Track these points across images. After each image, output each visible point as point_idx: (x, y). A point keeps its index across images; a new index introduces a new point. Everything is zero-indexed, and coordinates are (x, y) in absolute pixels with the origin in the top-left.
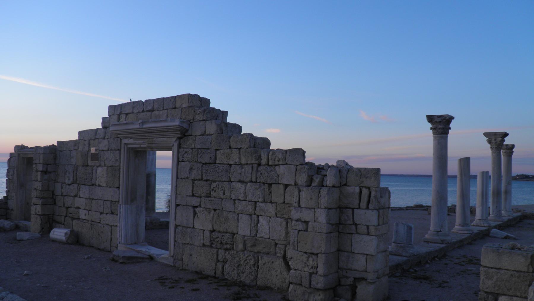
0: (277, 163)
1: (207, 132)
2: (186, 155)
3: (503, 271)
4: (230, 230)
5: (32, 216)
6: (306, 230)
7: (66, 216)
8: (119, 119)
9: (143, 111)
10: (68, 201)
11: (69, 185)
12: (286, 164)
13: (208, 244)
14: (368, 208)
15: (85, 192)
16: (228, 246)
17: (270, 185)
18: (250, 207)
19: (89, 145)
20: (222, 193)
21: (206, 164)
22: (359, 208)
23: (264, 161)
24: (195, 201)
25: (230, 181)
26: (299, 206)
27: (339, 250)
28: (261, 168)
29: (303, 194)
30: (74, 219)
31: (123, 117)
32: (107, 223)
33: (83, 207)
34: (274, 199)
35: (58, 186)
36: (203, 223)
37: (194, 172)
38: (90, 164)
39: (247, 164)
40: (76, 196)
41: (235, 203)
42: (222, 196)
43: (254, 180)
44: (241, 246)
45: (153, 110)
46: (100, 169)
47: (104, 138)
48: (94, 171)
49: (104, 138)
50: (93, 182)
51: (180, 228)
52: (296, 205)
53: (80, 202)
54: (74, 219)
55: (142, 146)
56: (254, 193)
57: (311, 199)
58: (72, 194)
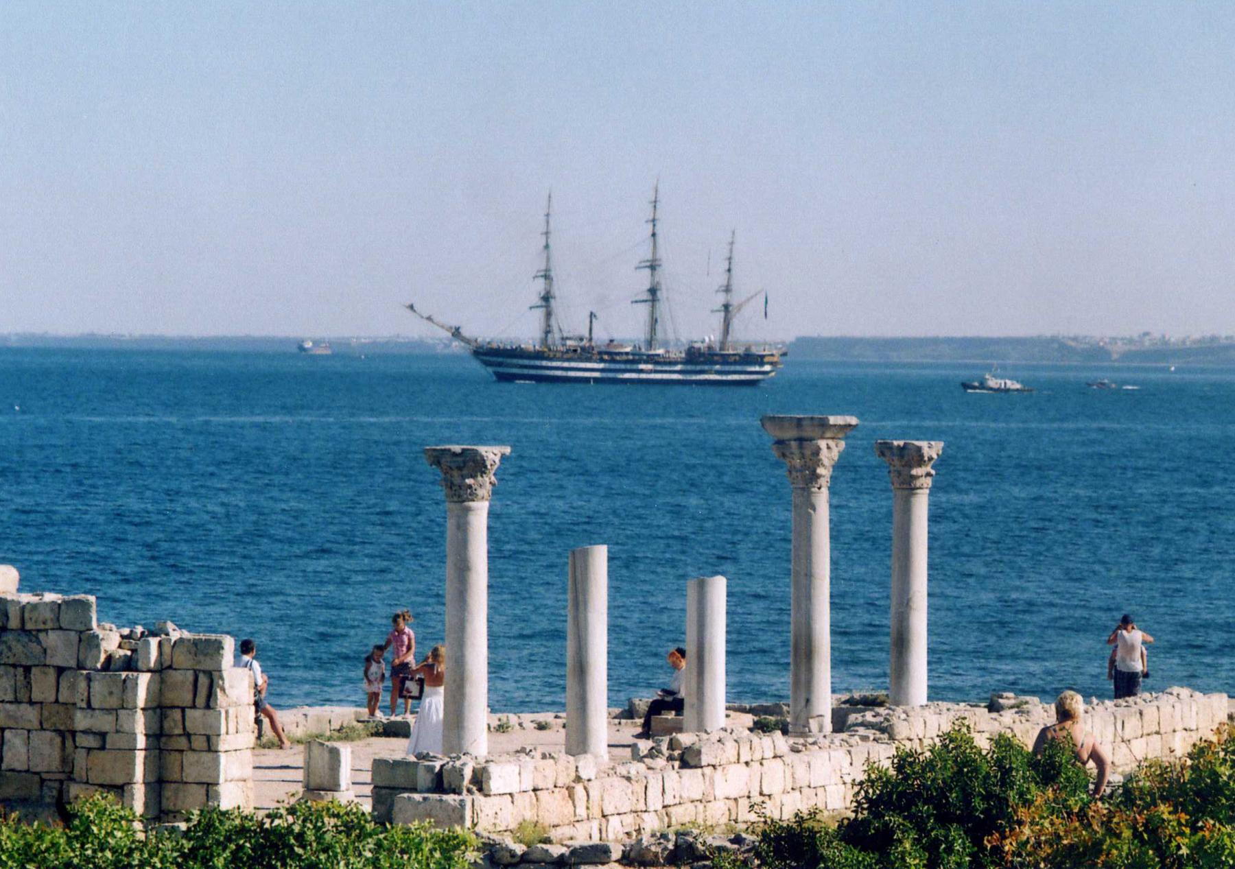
0: (42, 627)
6: (103, 748)
12: (61, 628)
17: (27, 669)
22: (194, 707)
26: (89, 706)
29: (96, 686)
34: (36, 696)
52: (84, 705)
57: (111, 693)
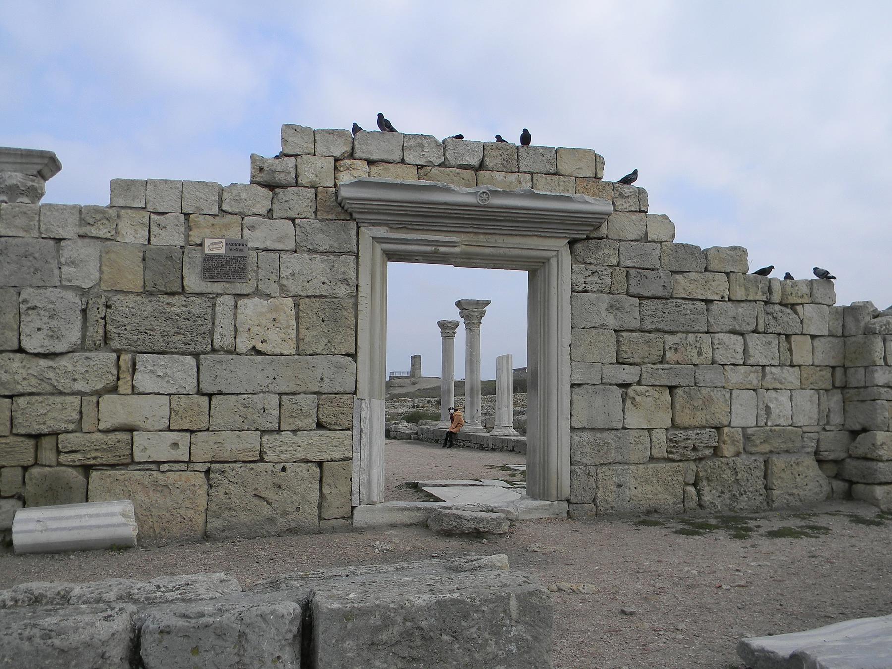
2: (595, 278)
23: (776, 297)
24: (628, 374)
28: (770, 308)
32: (300, 455)
34: (797, 360)
36: (649, 414)
39: (746, 301)
40: (113, 390)
42: (695, 360)
43: (761, 328)
56: (762, 350)
58: (79, 386)
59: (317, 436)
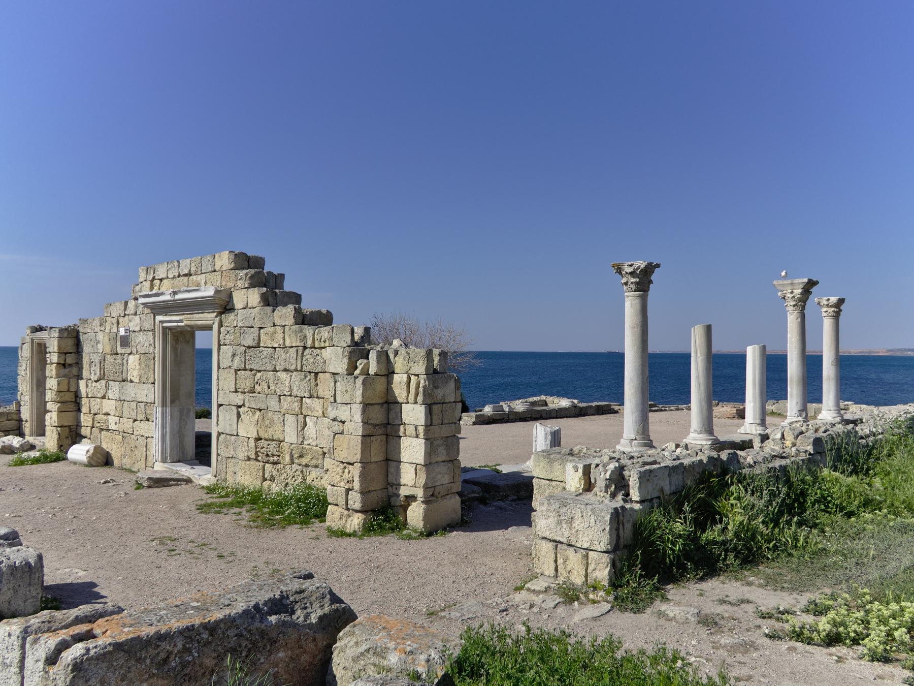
0: (323, 345)
1: (250, 305)
3: (554, 483)
4: (276, 437)
5: (47, 428)
7: (93, 427)
8: (152, 288)
9: (179, 276)
10: (95, 405)
11: (96, 381)
13: (253, 456)
14: (416, 403)
15: (114, 390)
16: (275, 458)
17: (316, 374)
18: (296, 404)
19: (118, 323)
20: (266, 387)
21: (249, 347)
22: (407, 403)
24: (238, 399)
25: (275, 370)
26: (335, 401)
27: (387, 460)
28: (307, 351)
30: (102, 429)
31: (157, 282)
33: (112, 413)
34: (321, 393)
35: (82, 383)
37: (237, 359)
38: (119, 352)
40: (104, 397)
41: (280, 400)
44: (287, 458)
45: (189, 275)
46: (131, 357)
47: (135, 314)
48: (125, 361)
49: (135, 314)
50: (124, 376)
51: (222, 436)
53: (109, 406)
54: (102, 429)
55: (180, 324)
56: (299, 385)
57: (347, 391)
59: (144, 425)
